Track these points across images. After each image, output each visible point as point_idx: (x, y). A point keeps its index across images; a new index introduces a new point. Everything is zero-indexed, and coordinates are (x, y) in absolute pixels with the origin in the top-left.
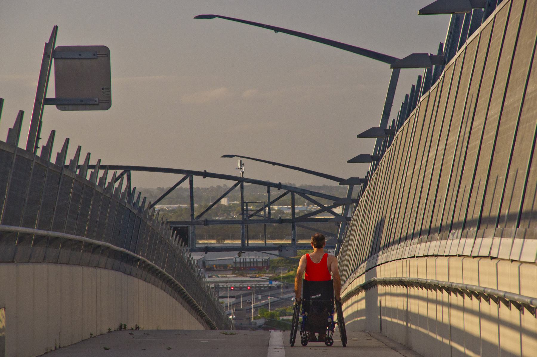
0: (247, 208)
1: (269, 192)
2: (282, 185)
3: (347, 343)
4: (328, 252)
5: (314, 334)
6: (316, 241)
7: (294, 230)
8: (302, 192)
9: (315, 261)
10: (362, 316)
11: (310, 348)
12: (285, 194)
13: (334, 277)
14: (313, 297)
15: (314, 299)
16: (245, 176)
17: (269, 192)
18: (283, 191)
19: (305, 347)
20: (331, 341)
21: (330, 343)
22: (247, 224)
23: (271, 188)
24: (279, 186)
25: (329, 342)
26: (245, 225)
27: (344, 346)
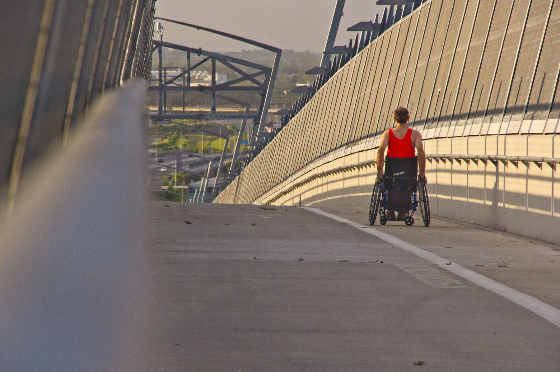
1: (188, 57)
3: (429, 223)
4: (274, 122)
5: (394, 213)
6: (399, 116)
7: (214, 99)
8: (223, 58)
9: (399, 136)
10: (368, 192)
11: (401, 227)
12: (205, 60)
13: (419, 154)
14: (395, 174)
15: (396, 176)
16: (164, 40)
17: (188, 57)
18: (202, 57)
19: (409, 228)
20: (412, 220)
21: (410, 222)
22: (164, 91)
24: (199, 52)
25: (410, 222)
27: (427, 225)
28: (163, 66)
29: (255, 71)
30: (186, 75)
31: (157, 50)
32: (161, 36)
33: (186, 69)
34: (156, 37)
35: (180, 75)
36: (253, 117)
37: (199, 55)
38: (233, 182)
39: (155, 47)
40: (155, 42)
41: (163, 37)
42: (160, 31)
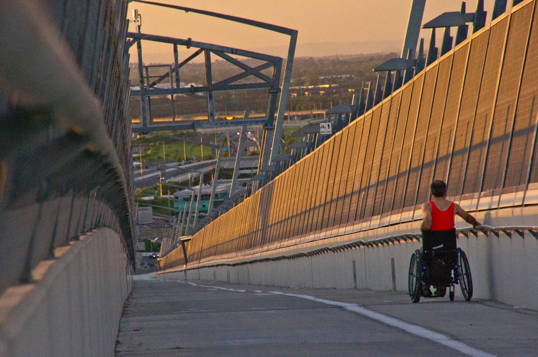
2: (193, 42)
8: (220, 49)
12: (196, 54)
18: (193, 50)
22: (148, 95)
24: (188, 43)
31: (135, 45)
32: (139, 27)
34: (132, 28)
35: (167, 75)
36: (262, 121)
37: (188, 47)
38: (240, 204)
39: (132, 41)
40: (132, 35)
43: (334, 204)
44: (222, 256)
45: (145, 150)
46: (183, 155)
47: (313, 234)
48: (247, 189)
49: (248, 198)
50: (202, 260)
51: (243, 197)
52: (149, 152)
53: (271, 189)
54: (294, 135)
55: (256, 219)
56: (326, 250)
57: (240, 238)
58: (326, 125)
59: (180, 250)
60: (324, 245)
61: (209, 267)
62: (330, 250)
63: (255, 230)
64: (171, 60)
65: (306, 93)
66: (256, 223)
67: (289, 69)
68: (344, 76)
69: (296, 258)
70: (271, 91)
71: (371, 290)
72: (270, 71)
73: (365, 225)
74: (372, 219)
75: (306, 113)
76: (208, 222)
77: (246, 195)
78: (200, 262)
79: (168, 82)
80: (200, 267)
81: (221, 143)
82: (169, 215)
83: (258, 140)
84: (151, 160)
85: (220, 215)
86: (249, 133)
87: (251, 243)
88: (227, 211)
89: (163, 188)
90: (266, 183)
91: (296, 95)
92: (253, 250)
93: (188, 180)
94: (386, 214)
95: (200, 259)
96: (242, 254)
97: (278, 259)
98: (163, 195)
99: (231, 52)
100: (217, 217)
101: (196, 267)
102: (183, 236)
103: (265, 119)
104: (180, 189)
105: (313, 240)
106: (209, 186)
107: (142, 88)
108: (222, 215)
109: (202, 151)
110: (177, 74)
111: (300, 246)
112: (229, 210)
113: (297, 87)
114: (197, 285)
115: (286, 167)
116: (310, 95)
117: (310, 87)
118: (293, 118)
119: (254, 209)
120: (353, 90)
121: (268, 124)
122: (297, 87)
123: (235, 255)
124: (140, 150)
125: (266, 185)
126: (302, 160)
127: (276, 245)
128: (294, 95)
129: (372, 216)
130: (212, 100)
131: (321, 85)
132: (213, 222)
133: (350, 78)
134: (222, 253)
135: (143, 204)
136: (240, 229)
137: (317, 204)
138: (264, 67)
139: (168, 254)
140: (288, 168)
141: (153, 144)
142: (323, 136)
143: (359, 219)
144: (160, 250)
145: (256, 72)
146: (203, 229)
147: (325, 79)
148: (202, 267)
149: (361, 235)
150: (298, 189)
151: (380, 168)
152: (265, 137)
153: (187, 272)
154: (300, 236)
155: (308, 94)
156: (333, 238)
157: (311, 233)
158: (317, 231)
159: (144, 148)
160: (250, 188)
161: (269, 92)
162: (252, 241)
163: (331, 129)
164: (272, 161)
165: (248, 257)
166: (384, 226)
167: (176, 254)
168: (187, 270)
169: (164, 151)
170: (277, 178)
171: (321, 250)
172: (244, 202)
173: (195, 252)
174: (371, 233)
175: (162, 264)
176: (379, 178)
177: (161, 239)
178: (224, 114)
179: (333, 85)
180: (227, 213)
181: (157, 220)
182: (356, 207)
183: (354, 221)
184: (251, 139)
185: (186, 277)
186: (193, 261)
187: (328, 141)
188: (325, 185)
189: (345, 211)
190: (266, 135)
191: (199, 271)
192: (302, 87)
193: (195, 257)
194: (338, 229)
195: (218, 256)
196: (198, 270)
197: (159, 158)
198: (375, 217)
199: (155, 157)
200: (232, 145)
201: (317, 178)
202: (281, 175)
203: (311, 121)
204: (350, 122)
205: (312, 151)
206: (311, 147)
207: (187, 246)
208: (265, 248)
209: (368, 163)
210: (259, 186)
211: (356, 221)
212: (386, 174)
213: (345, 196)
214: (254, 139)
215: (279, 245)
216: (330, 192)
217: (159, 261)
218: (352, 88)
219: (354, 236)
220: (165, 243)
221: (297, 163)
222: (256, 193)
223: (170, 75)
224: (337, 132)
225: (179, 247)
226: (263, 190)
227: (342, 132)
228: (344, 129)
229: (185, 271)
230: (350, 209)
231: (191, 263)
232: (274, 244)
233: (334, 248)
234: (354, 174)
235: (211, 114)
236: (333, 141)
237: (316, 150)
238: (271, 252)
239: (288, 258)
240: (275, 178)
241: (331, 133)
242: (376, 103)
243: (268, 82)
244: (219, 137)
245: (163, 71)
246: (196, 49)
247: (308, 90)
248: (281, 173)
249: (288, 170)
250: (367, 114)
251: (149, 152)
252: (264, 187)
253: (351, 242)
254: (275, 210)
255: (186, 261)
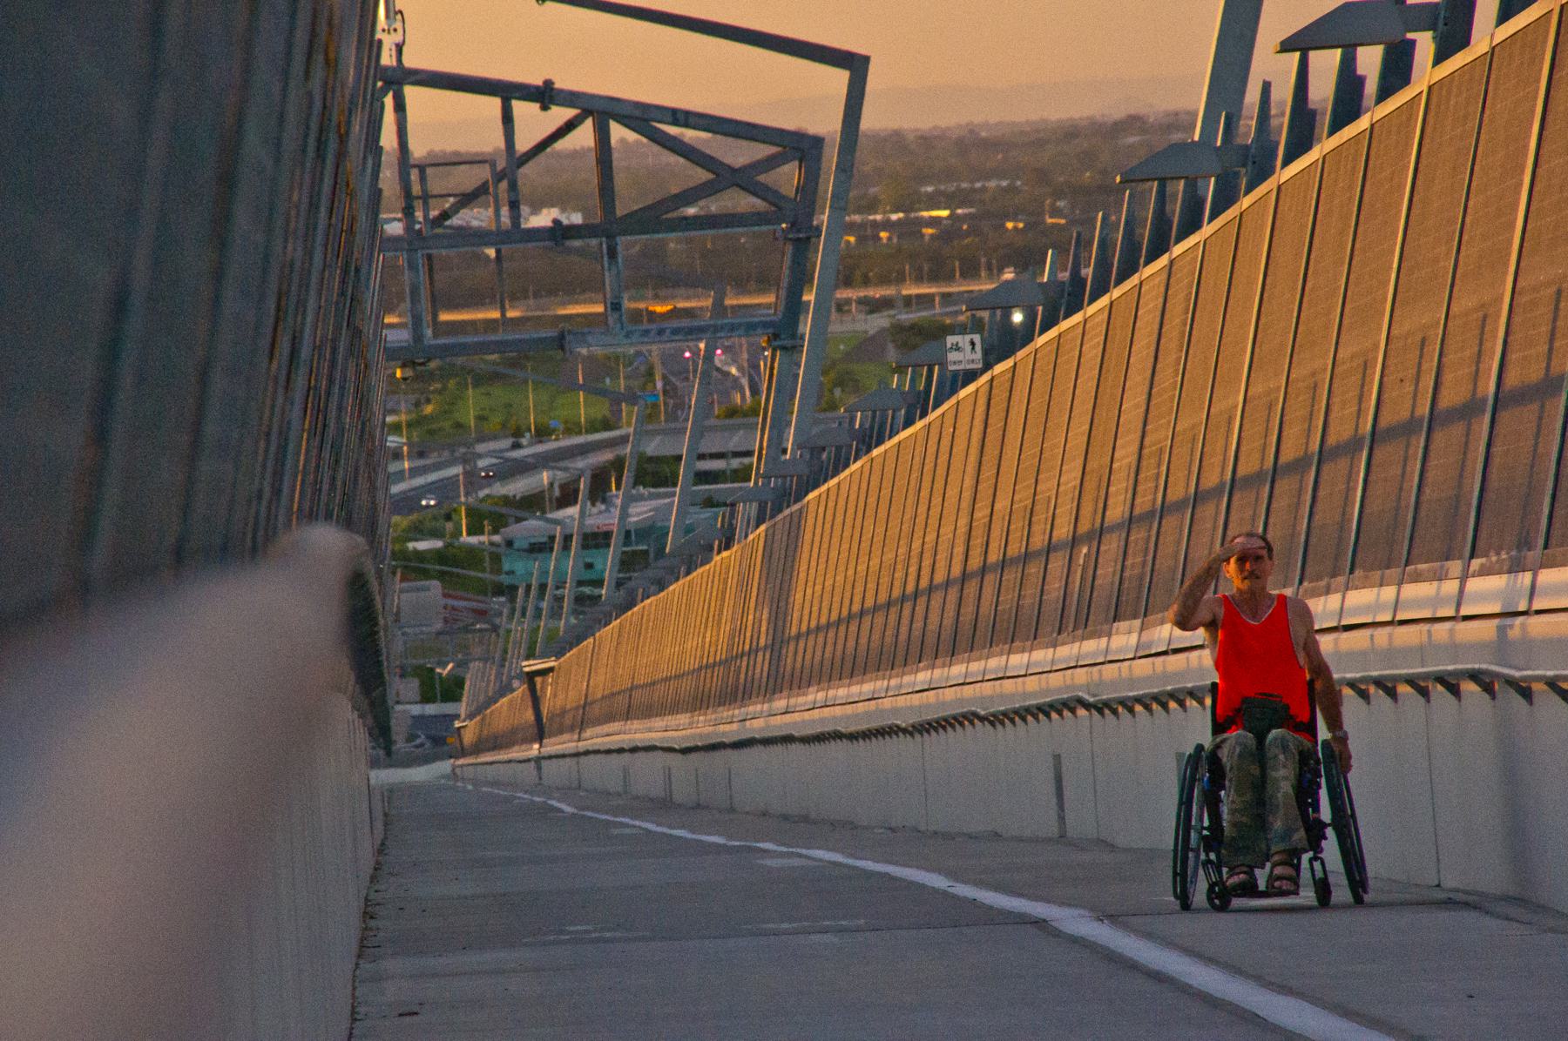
0: (424, 190)
1: (507, 118)
2: (561, 91)
7: (614, 268)
8: (637, 113)
12: (570, 126)
16: (410, 61)
17: (507, 118)
18: (561, 114)
23: (520, 108)
24: (545, 95)
26: (419, 255)
28: (412, 162)
29: (763, 151)
30: (504, 185)
33: (501, 165)
36: (765, 325)
37: (545, 108)
38: (700, 570)
41: (405, 49)
42: (393, 26)
43: (990, 579)
44: (648, 723)
45: (417, 404)
46: (527, 418)
47: (926, 668)
48: (722, 526)
49: (725, 554)
50: (588, 733)
51: (711, 548)
52: (428, 409)
53: (796, 524)
54: (848, 356)
55: (751, 617)
56: (970, 718)
57: (703, 671)
58: (963, 340)
59: (522, 700)
60: (961, 701)
61: (609, 752)
62: (982, 719)
63: (747, 647)
64: (494, 140)
65: (883, 235)
66: (749, 628)
67: (844, 171)
68: (992, 184)
69: (876, 737)
70: (791, 236)
71: (1112, 847)
72: (788, 177)
73: (1092, 647)
74: (1114, 630)
75: (883, 293)
76: (603, 622)
77: (720, 546)
78: (584, 735)
79: (486, 207)
80: (581, 750)
81: (636, 383)
82: (486, 595)
83: (744, 375)
84: (431, 433)
85: (640, 597)
86: (719, 352)
87: (737, 687)
88: (661, 590)
89: (471, 512)
90: (780, 511)
91: (852, 239)
92: (741, 707)
93: (543, 491)
94: (1160, 616)
95: (582, 730)
96: (708, 717)
97: (820, 738)
98: (469, 534)
99: (670, 120)
100: (631, 604)
101: (572, 751)
102: (527, 658)
103: (773, 318)
104: (519, 520)
105: (926, 687)
106: (603, 507)
107: (409, 228)
108: (648, 602)
109: (583, 407)
110: (513, 186)
111: (887, 703)
112: (668, 586)
113: (857, 218)
114: (576, 811)
115: (840, 464)
116: (895, 240)
117: (894, 217)
118: (846, 308)
119: (743, 584)
120: (1021, 225)
121: (783, 333)
122: (857, 218)
123: (687, 721)
124: (403, 403)
125: (780, 517)
126: (888, 444)
127: (814, 695)
128: (848, 242)
129: (1114, 622)
130: (617, 262)
131: (927, 210)
132: (618, 621)
133: (1011, 189)
134: (649, 711)
135: (415, 567)
136: (703, 646)
137: (940, 578)
138: (770, 163)
139: (486, 708)
140: (847, 466)
141: (438, 386)
142: (955, 374)
143: (1070, 629)
144: (462, 694)
145: (742, 179)
146: (591, 640)
147: (938, 193)
148: (587, 753)
149: (1081, 676)
150: (880, 530)
151: (1137, 474)
152: (775, 372)
153: (544, 763)
154: (888, 673)
155: (889, 239)
156: (992, 682)
157: (921, 665)
158: (939, 661)
159: (412, 398)
160: (731, 524)
161: (786, 239)
162: (738, 678)
163: (979, 355)
164: (799, 445)
165: (727, 728)
166: (1153, 652)
167: (511, 709)
168: (544, 758)
169: (471, 406)
170: (811, 496)
171: (955, 718)
172: (713, 563)
173: (568, 707)
174: (1110, 671)
175: (468, 737)
176: (1133, 505)
177: (461, 664)
178: (643, 298)
179: (959, 211)
180: (662, 594)
181: (454, 608)
182: (1062, 592)
183: (1055, 635)
184: (725, 368)
185: (540, 778)
186: (561, 732)
187: (971, 388)
188: (963, 522)
189: (1027, 602)
190: (776, 365)
191: (578, 763)
192: (871, 217)
193: (568, 720)
194: (1005, 657)
195: (635, 722)
196: (576, 759)
197: (459, 425)
198: (1123, 625)
199: (447, 425)
200: (668, 388)
201: (937, 500)
202: (824, 488)
203: (899, 317)
204: (1040, 334)
205: (921, 418)
206: (918, 406)
207: (543, 688)
208: (780, 704)
209: (1098, 462)
210: (758, 517)
211: (1064, 635)
212: (1155, 493)
213: (1027, 557)
214: (734, 371)
215: (821, 696)
216: (977, 542)
217: (459, 728)
218: (1015, 219)
219: (1055, 680)
220: (476, 680)
221: (875, 452)
222: (751, 537)
223: (491, 190)
224: (1000, 360)
225: (520, 690)
226: (771, 532)
227: (1015, 364)
228: (1021, 354)
229: (538, 760)
230: (1041, 595)
231: (553, 740)
232: (805, 694)
233: (993, 715)
234: (1055, 491)
235: (612, 303)
236: (987, 387)
237: (933, 416)
238: (796, 717)
239: (853, 737)
240: (806, 494)
241: (980, 366)
242: (1121, 279)
243: (780, 209)
244: (631, 364)
245: (469, 178)
246: (569, 113)
247: (887, 225)
248: (825, 481)
249: (847, 472)
250: (1091, 310)
251: (428, 409)
252: (772, 522)
253: (1048, 700)
254: (809, 591)
255: (540, 735)
